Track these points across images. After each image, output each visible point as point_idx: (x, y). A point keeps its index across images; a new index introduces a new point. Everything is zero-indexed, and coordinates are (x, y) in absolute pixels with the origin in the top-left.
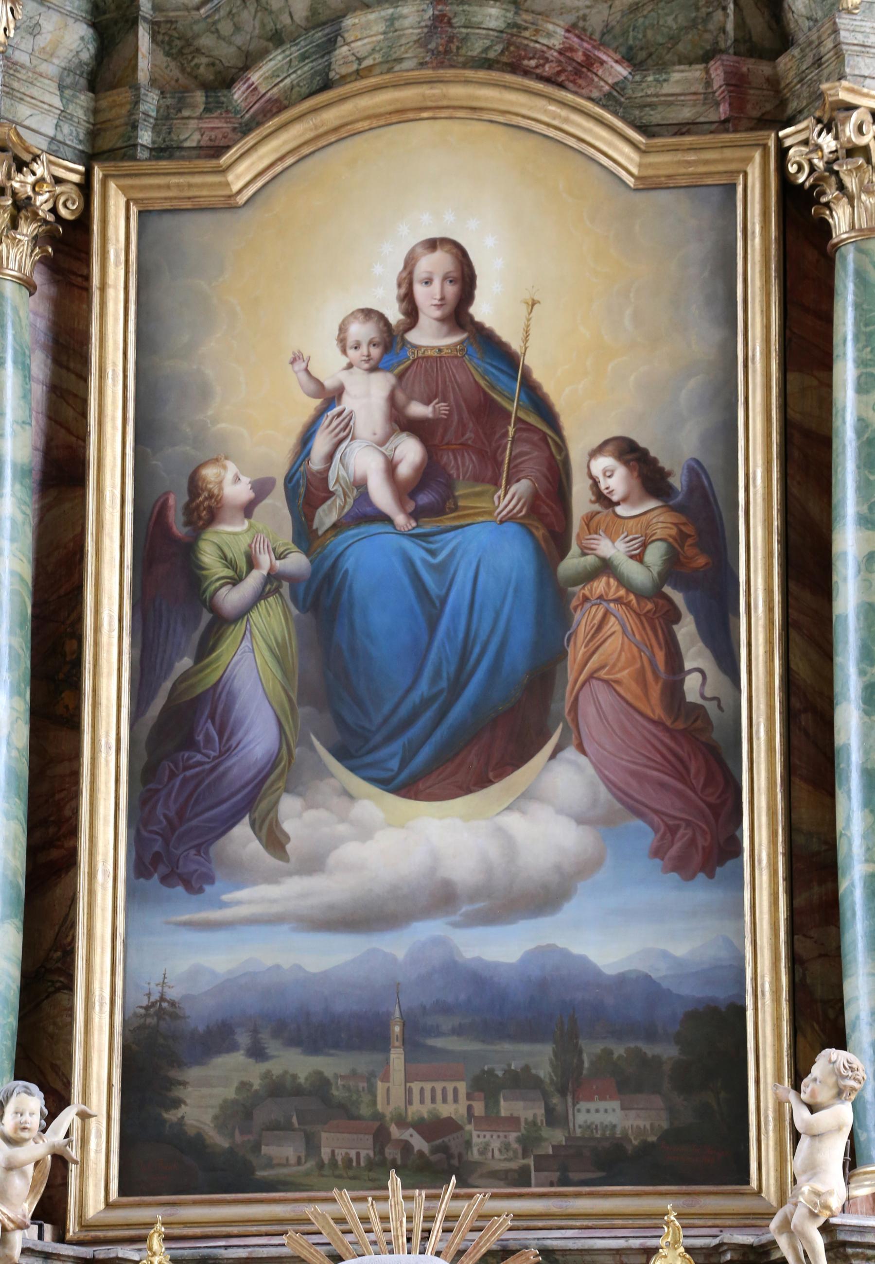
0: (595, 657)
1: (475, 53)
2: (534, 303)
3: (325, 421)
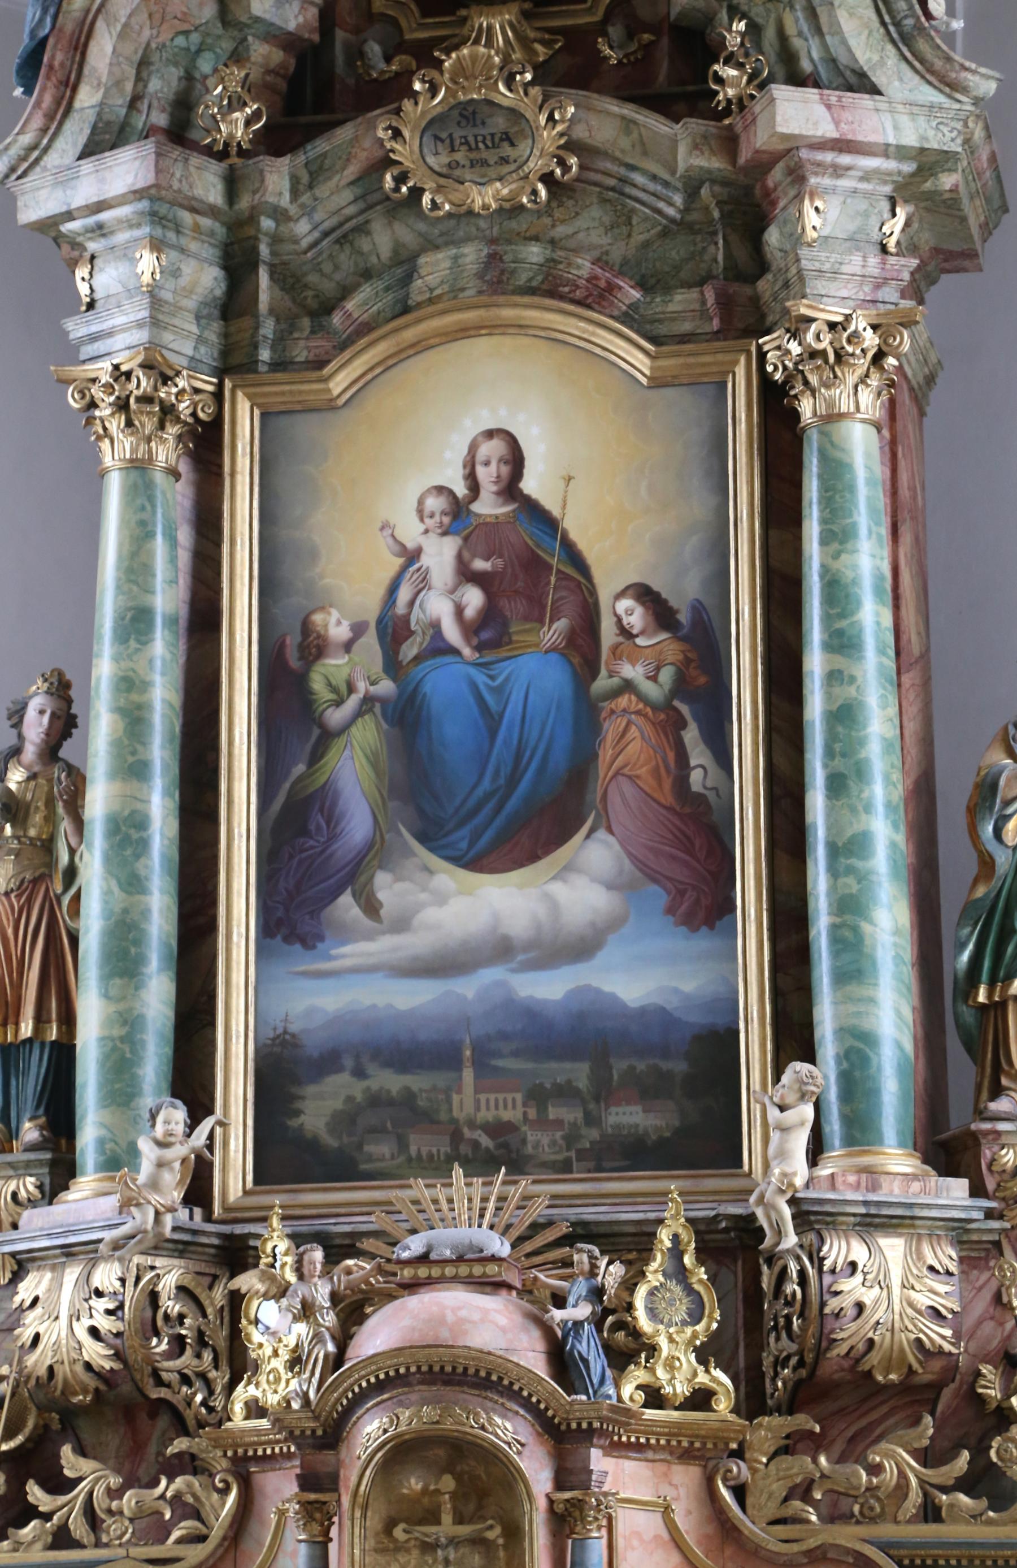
0: (620, 758)
1: (521, 283)
2: (570, 479)
3: (408, 576)
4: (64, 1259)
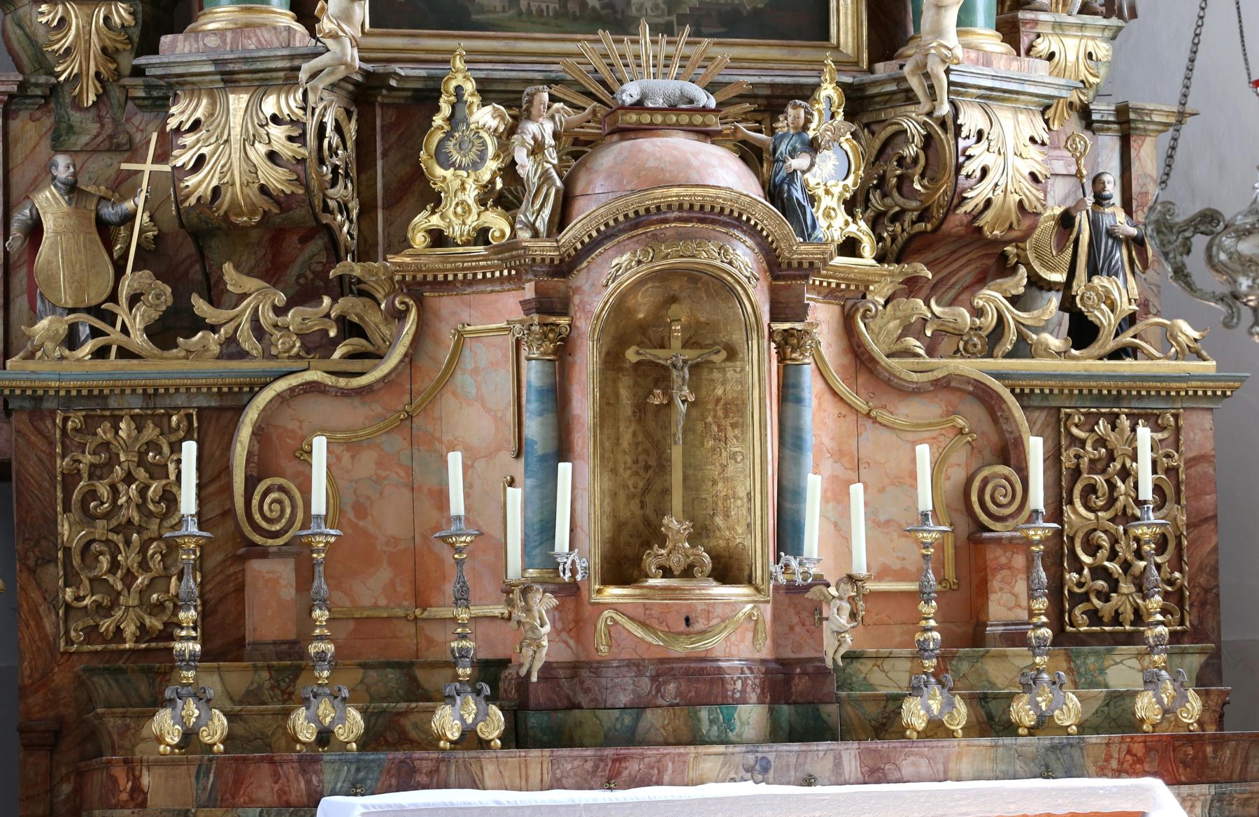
4: (221, 85)
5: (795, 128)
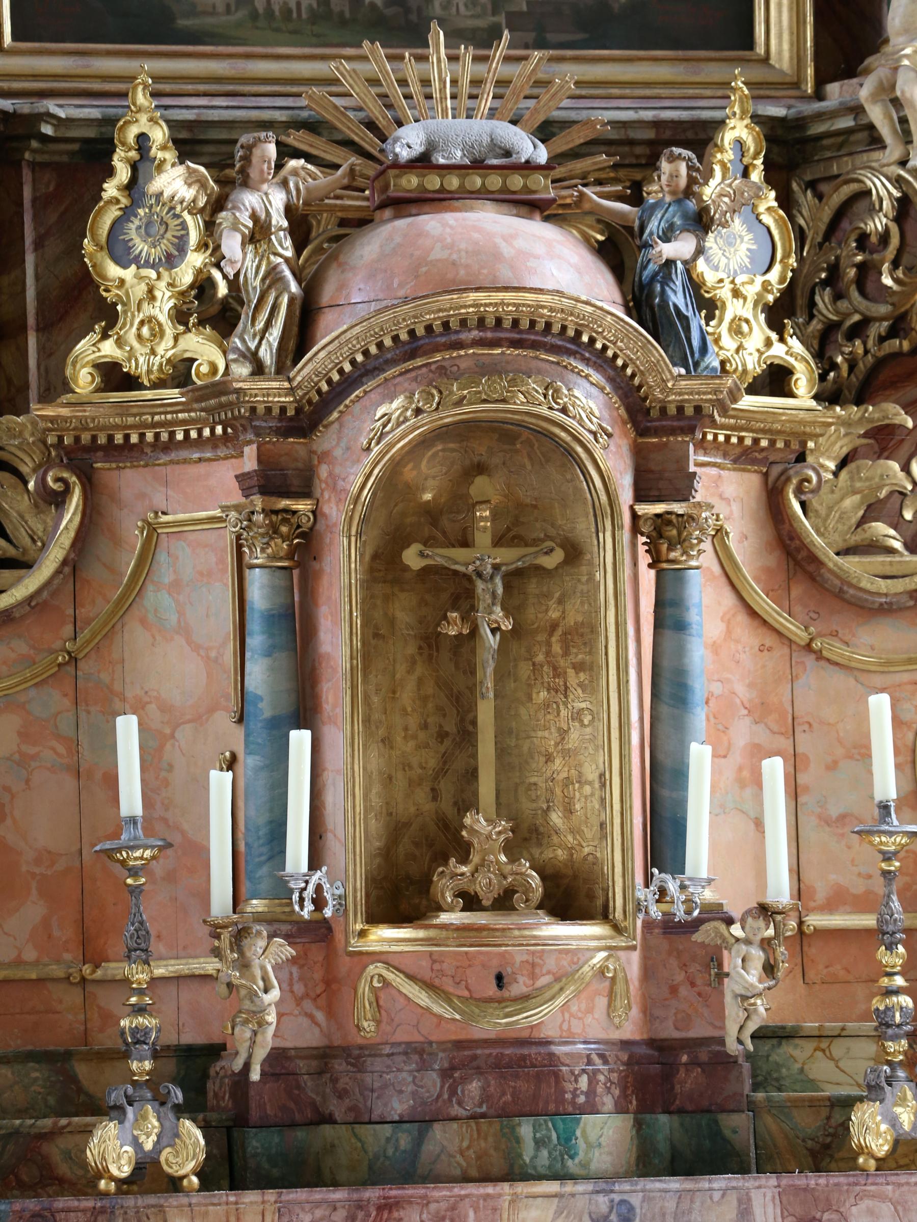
5: (673, 193)
